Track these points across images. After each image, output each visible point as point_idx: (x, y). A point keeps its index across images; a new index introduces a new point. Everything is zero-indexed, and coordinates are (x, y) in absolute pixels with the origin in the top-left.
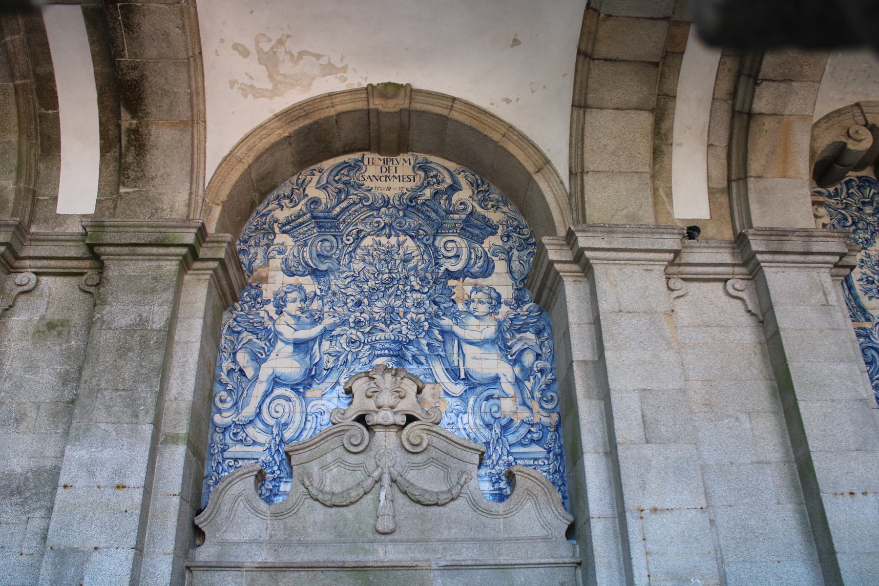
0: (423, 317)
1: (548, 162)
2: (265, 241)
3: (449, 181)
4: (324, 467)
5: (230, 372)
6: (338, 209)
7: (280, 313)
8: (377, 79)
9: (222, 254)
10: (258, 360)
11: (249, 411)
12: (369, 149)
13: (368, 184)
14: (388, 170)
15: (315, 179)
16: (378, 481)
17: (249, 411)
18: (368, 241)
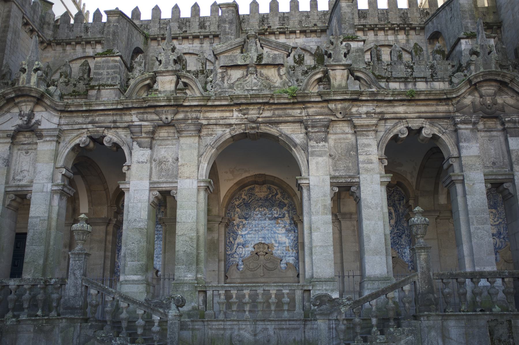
0: (269, 228)
1: (296, 194)
2: (233, 210)
3: (275, 192)
4: (250, 263)
5: (229, 242)
6: (249, 201)
7: (238, 228)
8: (256, 173)
9: (227, 221)
10: (235, 239)
11: (234, 251)
12: (256, 184)
13: (256, 194)
14: (261, 190)
15: (244, 193)
16: (261, 266)
17: (234, 251)
18: (257, 209)
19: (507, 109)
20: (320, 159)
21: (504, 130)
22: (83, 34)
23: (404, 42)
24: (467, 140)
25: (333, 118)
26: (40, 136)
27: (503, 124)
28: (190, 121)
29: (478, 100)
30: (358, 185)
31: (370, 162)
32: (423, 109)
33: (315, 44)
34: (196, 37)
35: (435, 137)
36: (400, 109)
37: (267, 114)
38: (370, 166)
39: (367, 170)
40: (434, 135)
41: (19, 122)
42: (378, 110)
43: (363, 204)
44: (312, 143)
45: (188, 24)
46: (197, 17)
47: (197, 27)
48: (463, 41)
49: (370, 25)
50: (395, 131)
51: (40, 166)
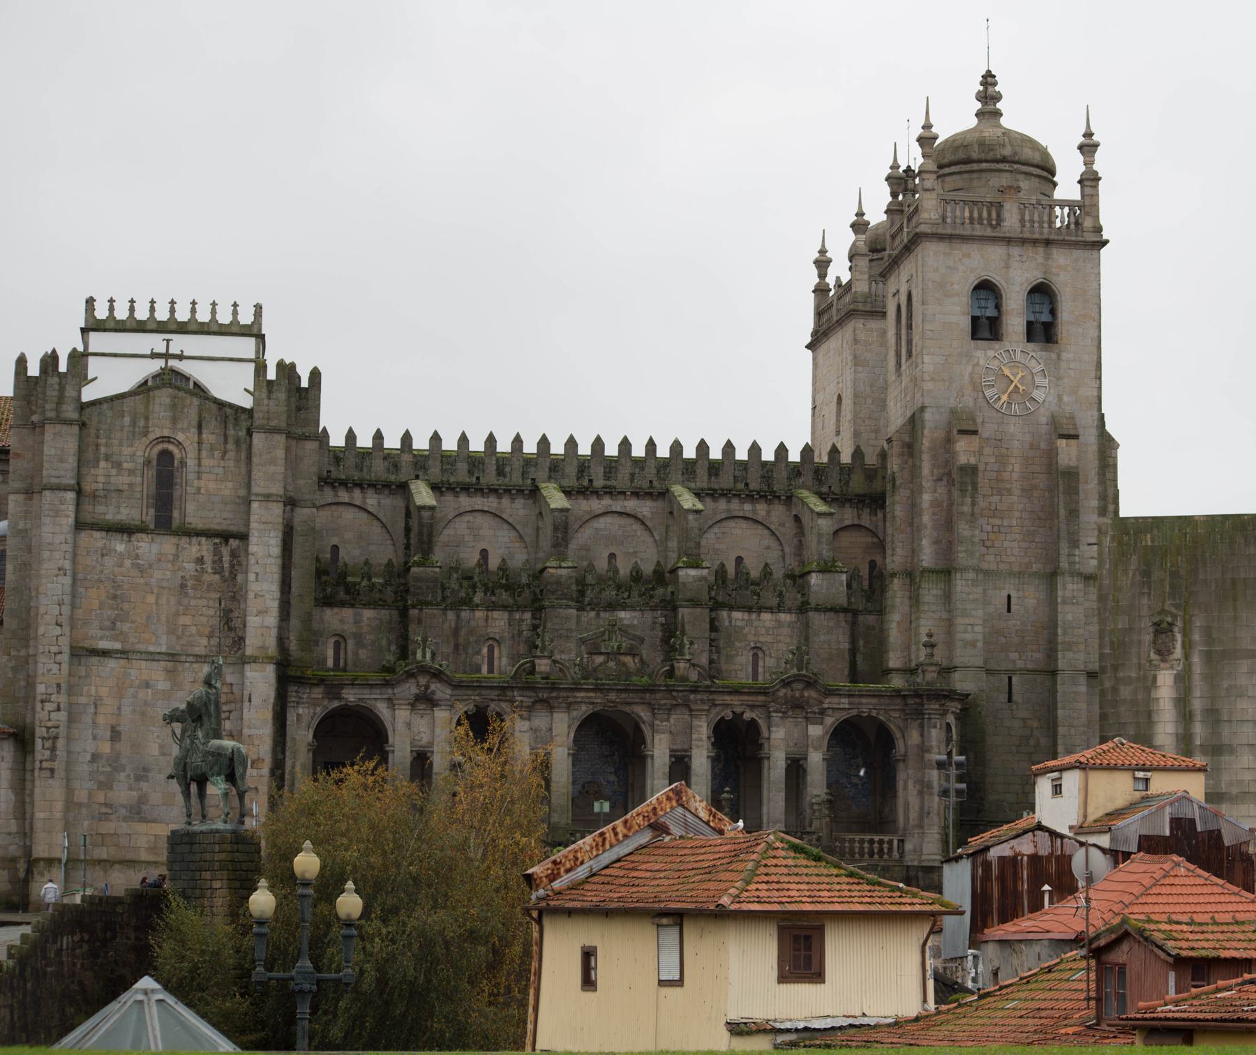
19: (811, 701)
20: (663, 736)
21: (807, 718)
22: (332, 468)
23: (764, 513)
24: (777, 726)
25: (675, 702)
26: (437, 705)
27: (807, 713)
28: (560, 700)
29: (789, 692)
30: (690, 757)
31: (701, 740)
32: (746, 698)
33: (648, 509)
34: (493, 491)
35: (753, 720)
36: (727, 698)
37: (624, 695)
38: (700, 743)
39: (698, 747)
40: (752, 719)
41: (414, 690)
42: (711, 697)
43: (693, 773)
44: (657, 722)
45: (481, 466)
46: (494, 458)
47: (494, 473)
48: (814, 575)
49: (723, 490)
50: (722, 714)
51: (438, 731)
